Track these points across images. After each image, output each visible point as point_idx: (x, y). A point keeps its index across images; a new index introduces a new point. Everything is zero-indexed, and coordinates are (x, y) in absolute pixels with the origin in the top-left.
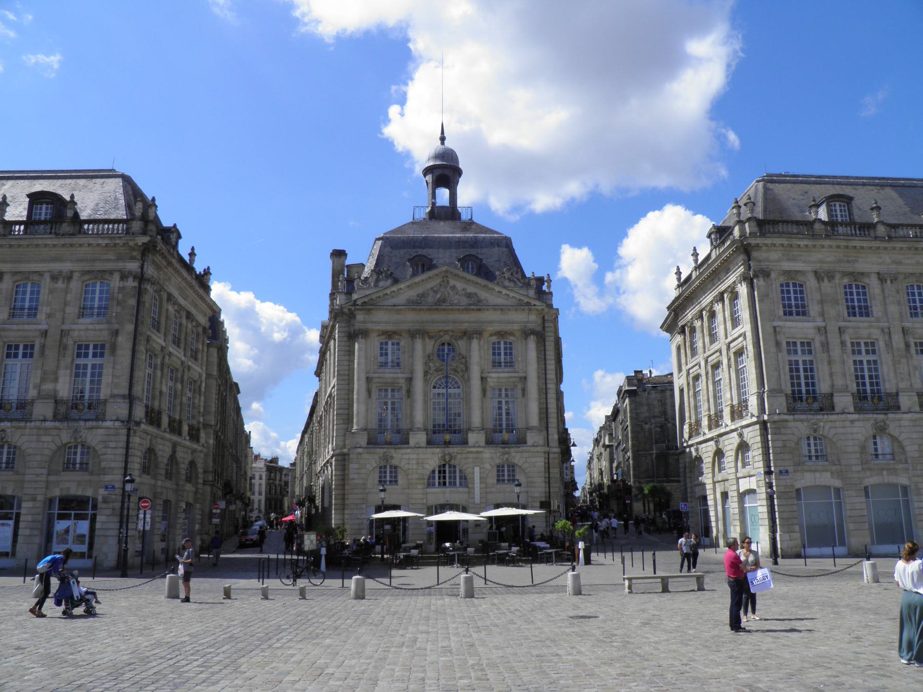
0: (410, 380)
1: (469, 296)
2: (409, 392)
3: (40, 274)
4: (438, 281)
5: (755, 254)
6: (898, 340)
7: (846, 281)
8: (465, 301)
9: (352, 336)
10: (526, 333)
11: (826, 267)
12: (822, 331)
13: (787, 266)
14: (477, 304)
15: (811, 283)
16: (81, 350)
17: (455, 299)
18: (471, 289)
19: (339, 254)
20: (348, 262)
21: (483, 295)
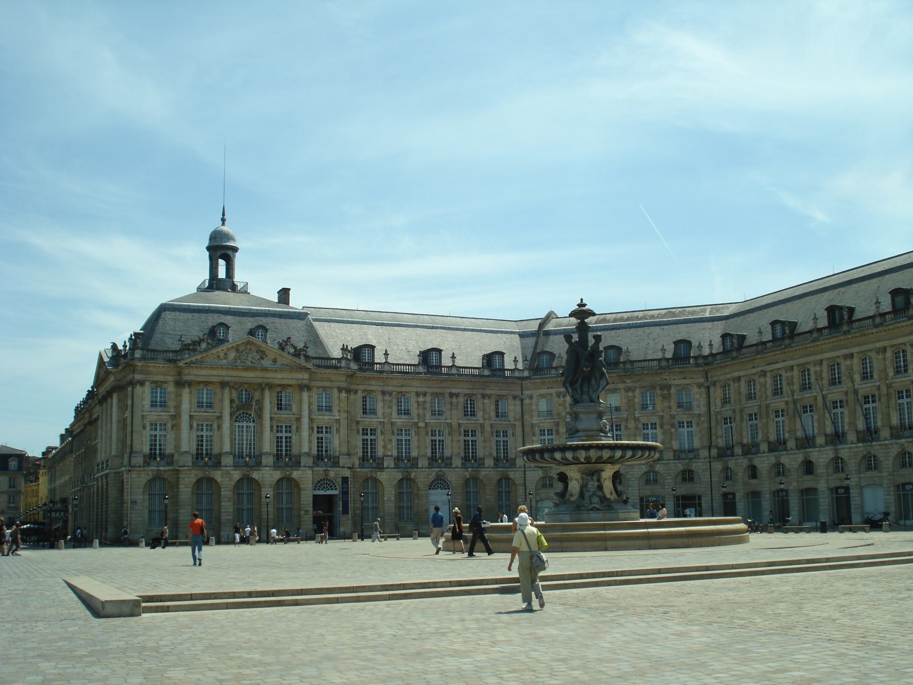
3: (904, 344)
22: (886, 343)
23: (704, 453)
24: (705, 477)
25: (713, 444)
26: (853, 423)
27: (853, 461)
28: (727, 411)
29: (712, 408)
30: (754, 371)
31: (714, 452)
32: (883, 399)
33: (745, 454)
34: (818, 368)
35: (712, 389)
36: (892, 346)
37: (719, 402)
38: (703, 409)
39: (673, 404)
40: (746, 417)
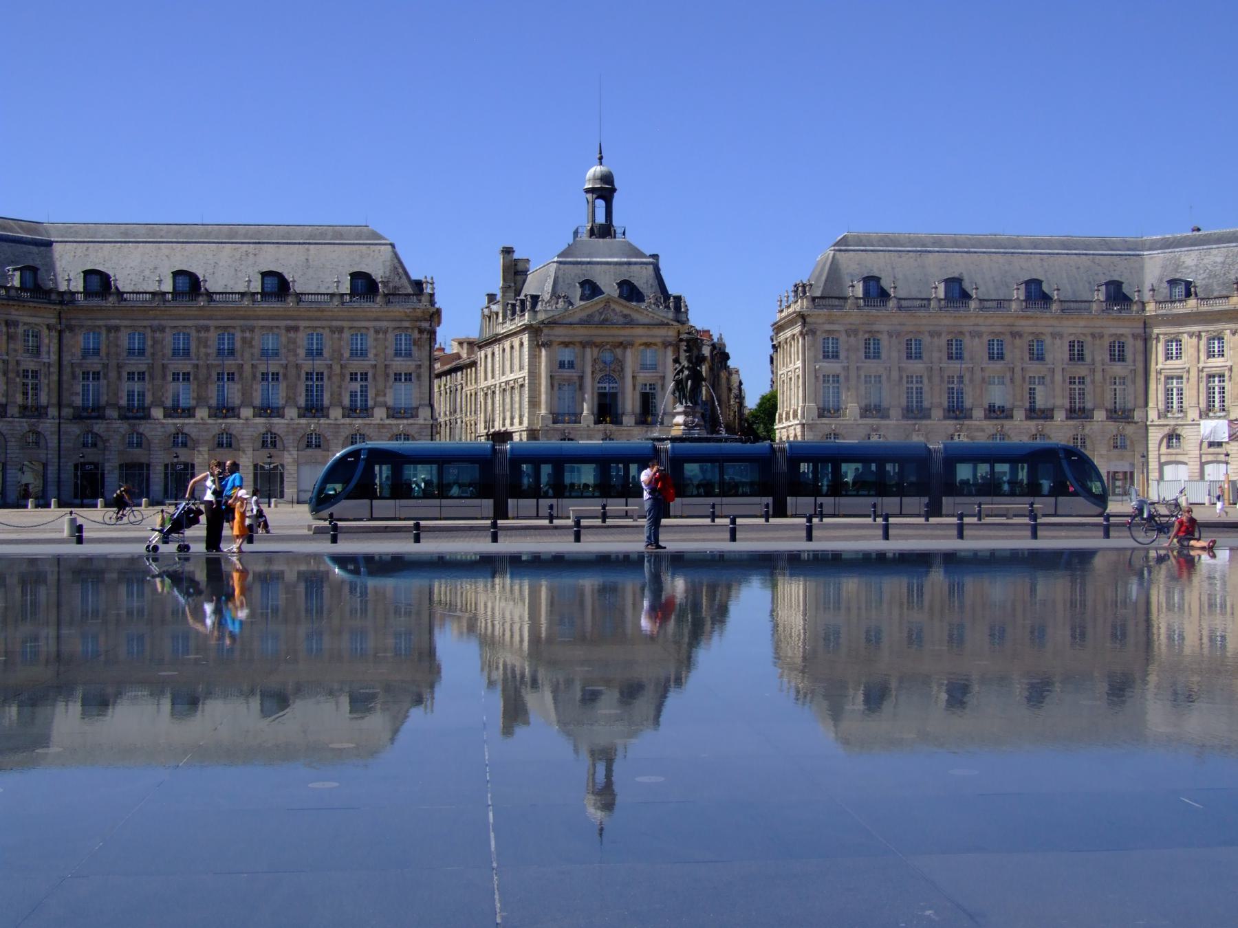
0: (581, 378)
1: (625, 316)
2: (581, 387)
4: (602, 305)
5: (808, 320)
6: (895, 375)
7: (866, 336)
8: (622, 320)
9: (536, 346)
10: (666, 345)
11: (853, 327)
12: (847, 369)
13: (828, 327)
14: (630, 323)
15: (843, 338)
16: (397, 377)
17: (615, 319)
18: (626, 311)
19: (508, 251)
20: (516, 256)
21: (635, 316)
22: (345, 324)
23: (53, 411)
24: (53, 442)
25: (65, 402)
26: (291, 400)
27: (291, 437)
28: (94, 364)
29: (67, 358)
30: (146, 323)
31: (67, 412)
32: (334, 379)
33: (123, 417)
34: (248, 335)
35: (67, 334)
36: (351, 328)
37: (78, 352)
38: (54, 357)
39: (19, 345)
40: (125, 375)
